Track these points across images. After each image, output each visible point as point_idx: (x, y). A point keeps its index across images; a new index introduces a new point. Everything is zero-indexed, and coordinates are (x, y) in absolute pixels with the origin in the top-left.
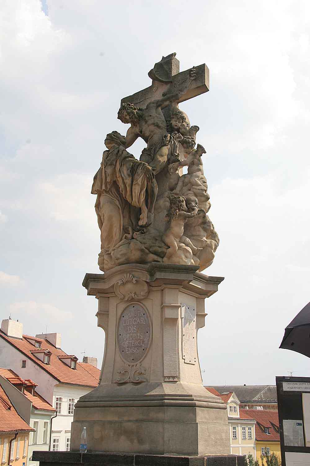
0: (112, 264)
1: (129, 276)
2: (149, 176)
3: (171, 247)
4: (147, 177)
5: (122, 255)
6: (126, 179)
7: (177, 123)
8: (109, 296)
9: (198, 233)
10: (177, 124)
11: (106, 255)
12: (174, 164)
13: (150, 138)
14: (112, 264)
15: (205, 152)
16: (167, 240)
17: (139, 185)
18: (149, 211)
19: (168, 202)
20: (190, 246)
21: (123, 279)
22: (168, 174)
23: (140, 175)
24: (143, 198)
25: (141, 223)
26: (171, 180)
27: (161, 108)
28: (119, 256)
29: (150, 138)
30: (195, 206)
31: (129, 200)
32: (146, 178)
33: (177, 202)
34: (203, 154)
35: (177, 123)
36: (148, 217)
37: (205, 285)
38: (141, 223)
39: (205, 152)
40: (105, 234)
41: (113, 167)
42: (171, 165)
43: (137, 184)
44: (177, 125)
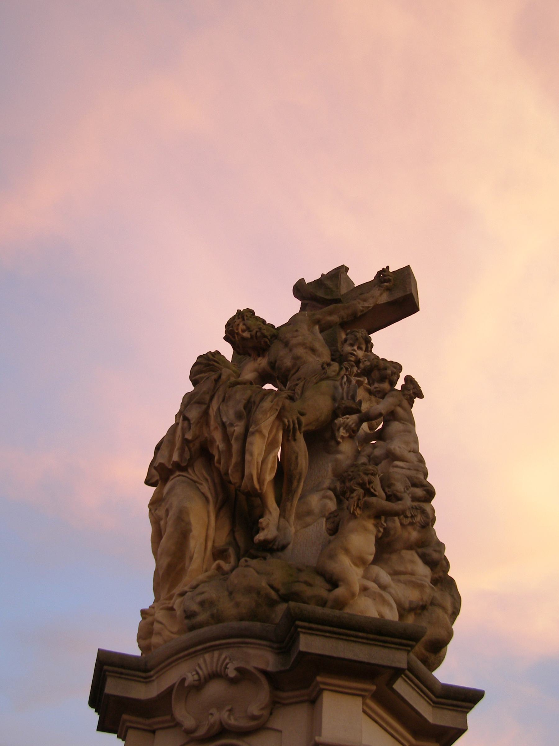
0: (172, 633)
1: (218, 660)
2: (288, 421)
3: (340, 583)
4: (284, 424)
5: (202, 604)
6: (231, 425)
7: (355, 348)
8: (155, 727)
9: (409, 567)
10: (356, 351)
11: (162, 609)
12: (348, 418)
13: (292, 372)
14: (172, 633)
15: (421, 396)
16: (333, 567)
17: (263, 436)
18: (283, 514)
19: (330, 499)
20: (393, 591)
21: (201, 668)
22: (333, 443)
23: (268, 415)
24: (269, 476)
25: (260, 537)
26: (339, 456)
27: (319, 328)
28: (195, 607)
29: (292, 372)
30: (405, 492)
31: (234, 478)
32: (281, 427)
33: (361, 473)
34: (417, 400)
35: (355, 348)
36: (278, 528)
37: (430, 708)
38: (260, 537)
39: (421, 396)
40: (165, 561)
41: (204, 407)
42: (340, 420)
43: (260, 432)
44: (355, 353)
